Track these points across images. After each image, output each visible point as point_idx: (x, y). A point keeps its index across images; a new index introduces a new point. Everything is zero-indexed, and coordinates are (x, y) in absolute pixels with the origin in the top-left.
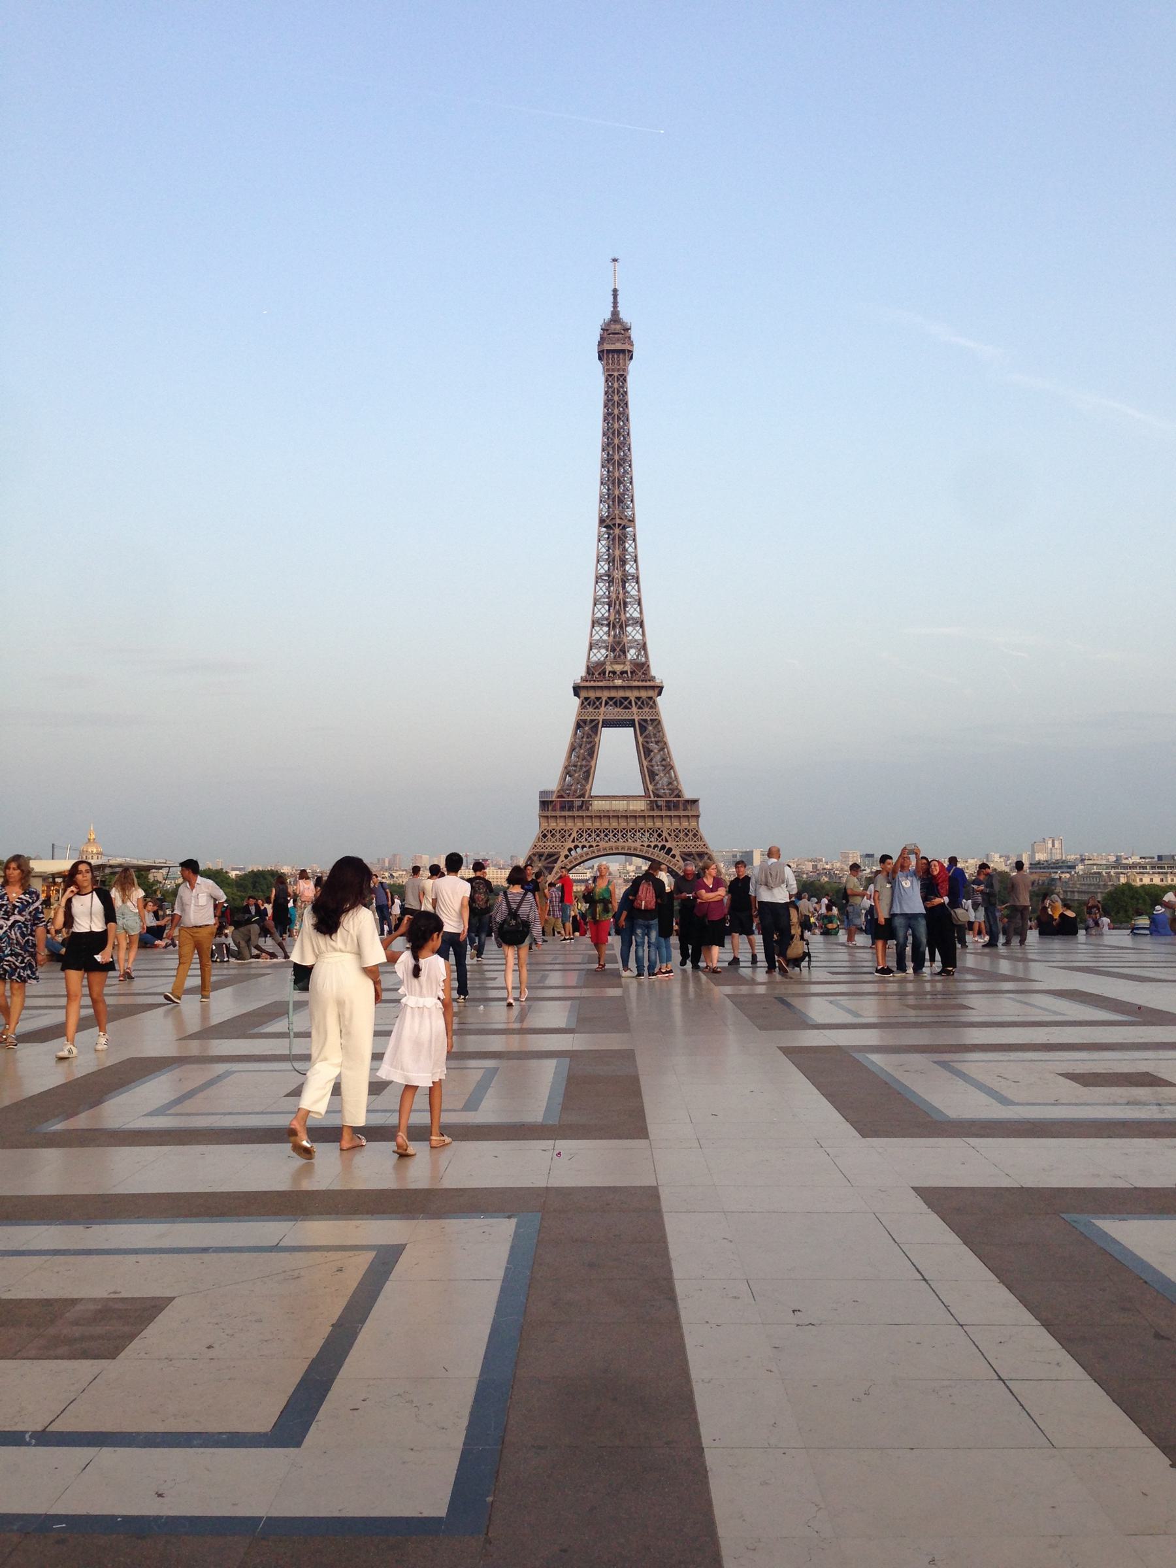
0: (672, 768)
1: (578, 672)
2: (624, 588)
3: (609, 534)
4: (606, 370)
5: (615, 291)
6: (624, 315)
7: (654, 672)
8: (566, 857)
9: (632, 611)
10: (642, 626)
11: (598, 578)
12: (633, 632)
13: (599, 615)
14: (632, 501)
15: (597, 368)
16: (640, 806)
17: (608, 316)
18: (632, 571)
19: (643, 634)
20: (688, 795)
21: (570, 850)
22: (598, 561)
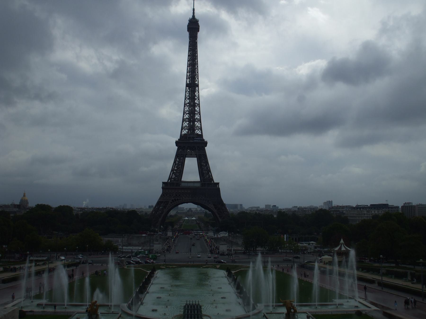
0: (210, 172)
1: (177, 138)
2: (195, 108)
3: (189, 89)
4: (190, 34)
5: (194, 9)
6: (196, 17)
7: (204, 138)
8: (171, 203)
9: (197, 117)
10: (201, 122)
11: (185, 105)
12: (197, 124)
13: (185, 117)
14: (198, 79)
15: (187, 34)
16: (198, 185)
17: (191, 17)
18: (198, 102)
19: (201, 125)
20: (216, 181)
21: (173, 200)
22: (185, 99)
